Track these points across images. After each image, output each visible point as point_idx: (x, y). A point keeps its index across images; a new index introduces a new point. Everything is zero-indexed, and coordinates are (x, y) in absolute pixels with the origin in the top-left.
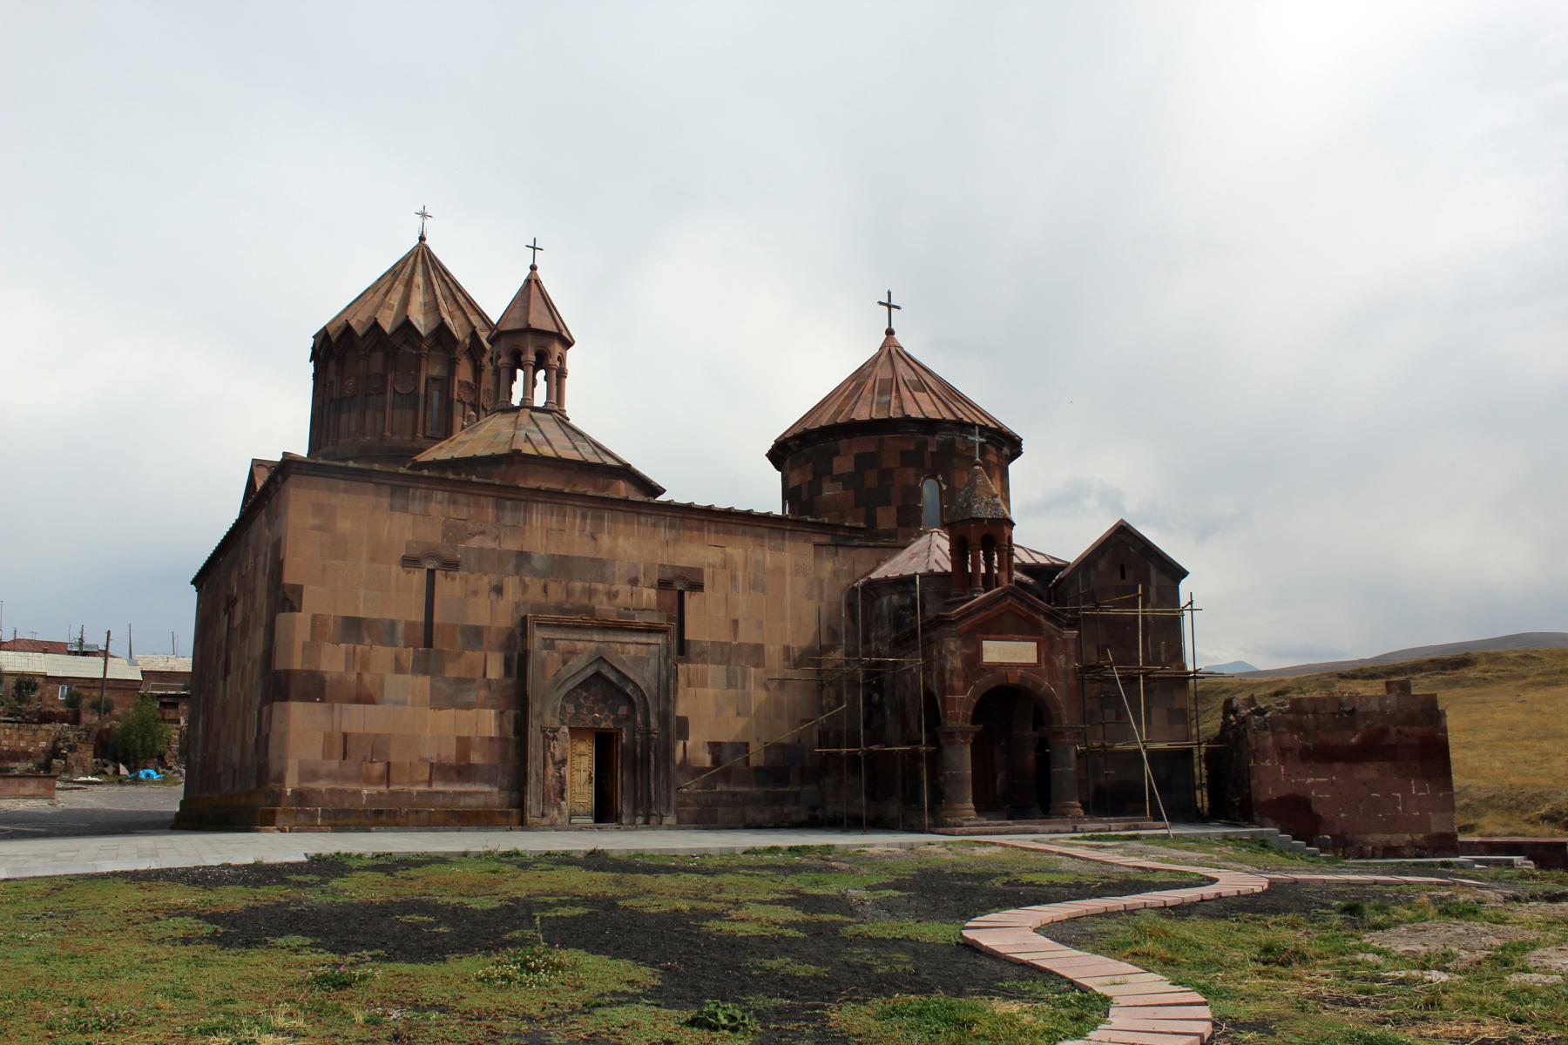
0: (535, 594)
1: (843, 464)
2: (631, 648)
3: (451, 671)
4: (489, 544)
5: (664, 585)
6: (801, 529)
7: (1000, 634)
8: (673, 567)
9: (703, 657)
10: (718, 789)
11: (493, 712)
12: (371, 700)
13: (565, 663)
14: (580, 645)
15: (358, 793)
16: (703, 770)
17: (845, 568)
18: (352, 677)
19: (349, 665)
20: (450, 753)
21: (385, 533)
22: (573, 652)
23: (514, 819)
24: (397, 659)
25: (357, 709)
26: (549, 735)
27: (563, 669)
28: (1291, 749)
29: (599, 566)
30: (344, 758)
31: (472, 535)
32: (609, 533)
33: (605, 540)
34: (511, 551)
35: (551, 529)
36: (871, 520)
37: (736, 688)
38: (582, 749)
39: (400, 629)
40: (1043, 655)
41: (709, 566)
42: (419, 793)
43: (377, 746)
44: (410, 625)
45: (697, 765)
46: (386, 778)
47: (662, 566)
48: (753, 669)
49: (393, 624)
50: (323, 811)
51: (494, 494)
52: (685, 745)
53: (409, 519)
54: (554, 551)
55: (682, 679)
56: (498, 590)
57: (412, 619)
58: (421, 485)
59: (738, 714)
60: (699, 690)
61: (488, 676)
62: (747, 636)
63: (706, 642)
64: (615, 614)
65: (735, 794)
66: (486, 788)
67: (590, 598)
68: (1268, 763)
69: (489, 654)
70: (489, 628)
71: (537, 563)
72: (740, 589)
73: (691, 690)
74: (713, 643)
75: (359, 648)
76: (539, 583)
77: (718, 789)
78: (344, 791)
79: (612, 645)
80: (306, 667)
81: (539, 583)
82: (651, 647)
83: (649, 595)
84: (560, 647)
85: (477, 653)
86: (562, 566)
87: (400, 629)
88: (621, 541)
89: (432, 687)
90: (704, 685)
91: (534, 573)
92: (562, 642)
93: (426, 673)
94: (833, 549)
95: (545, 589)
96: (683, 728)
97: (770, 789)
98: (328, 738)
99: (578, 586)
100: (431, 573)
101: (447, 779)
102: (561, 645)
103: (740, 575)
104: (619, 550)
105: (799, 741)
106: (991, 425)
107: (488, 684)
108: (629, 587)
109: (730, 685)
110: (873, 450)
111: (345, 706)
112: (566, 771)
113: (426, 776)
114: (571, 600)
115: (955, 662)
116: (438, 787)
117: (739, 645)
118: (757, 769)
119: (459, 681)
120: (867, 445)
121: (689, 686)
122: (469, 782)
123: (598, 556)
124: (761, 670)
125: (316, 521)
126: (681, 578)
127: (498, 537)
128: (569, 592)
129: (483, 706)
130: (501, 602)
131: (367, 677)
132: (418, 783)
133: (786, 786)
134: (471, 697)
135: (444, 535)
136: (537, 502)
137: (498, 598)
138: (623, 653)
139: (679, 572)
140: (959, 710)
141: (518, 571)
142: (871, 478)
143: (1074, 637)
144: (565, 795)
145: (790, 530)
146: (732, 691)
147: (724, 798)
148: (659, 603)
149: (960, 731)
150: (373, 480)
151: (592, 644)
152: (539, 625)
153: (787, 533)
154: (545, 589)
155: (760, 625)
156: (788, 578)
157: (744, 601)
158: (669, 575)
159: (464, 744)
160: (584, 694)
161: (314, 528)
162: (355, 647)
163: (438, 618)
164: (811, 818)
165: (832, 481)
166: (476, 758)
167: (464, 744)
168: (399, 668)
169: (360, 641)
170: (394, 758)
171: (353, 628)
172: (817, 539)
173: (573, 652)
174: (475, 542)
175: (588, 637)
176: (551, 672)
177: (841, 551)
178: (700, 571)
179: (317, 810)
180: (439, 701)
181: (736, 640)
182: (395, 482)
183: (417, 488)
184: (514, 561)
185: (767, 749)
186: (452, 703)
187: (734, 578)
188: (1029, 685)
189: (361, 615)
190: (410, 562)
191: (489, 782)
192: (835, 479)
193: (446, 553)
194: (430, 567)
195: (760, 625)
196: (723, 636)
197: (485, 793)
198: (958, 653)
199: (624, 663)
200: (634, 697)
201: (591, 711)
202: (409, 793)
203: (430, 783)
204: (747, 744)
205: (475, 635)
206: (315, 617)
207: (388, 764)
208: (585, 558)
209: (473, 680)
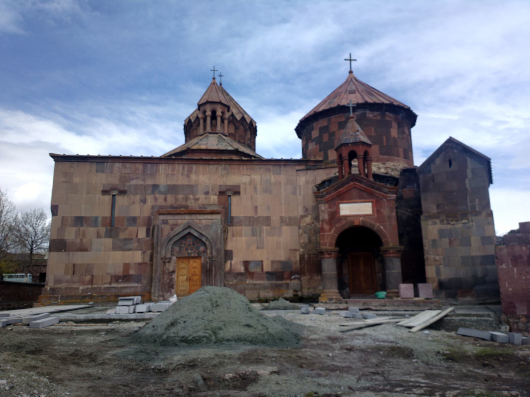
0: (161, 202)
1: (315, 134)
3: (122, 236)
4: (140, 182)
5: (222, 193)
7: (350, 200)
8: (226, 186)
9: (240, 224)
10: (248, 282)
11: (140, 252)
12: (86, 250)
13: (172, 229)
14: (180, 222)
15: (78, 288)
16: (240, 274)
17: (311, 179)
18: (78, 241)
20: (119, 271)
22: (176, 225)
25: (80, 254)
26: (166, 261)
28: (521, 257)
29: (191, 188)
31: (133, 179)
32: (195, 173)
33: (193, 177)
34: (149, 185)
35: (169, 174)
36: (326, 156)
37: (257, 236)
39: (100, 220)
41: (243, 184)
42: (105, 288)
43: (88, 269)
44: (104, 218)
46: (91, 282)
47: (220, 186)
48: (265, 228)
49: (96, 218)
50: (61, 296)
53: (104, 175)
54: (169, 183)
55: (230, 234)
56: (144, 201)
58: (109, 161)
59: (258, 248)
60: (238, 238)
62: (262, 213)
63: (242, 217)
65: (255, 285)
66: (136, 285)
67: (186, 202)
68: (504, 266)
70: (139, 217)
71: (162, 189)
72: (259, 193)
73: (235, 238)
74: (245, 217)
75: (81, 228)
76: (163, 196)
77: (248, 282)
78: (72, 288)
79: (195, 221)
80: (59, 238)
81: (163, 196)
83: (214, 198)
86: (173, 189)
87: (100, 220)
89: (113, 243)
90: (241, 235)
91: (160, 193)
92: (172, 221)
93: (110, 237)
94: (305, 172)
95: (165, 199)
96: (228, 255)
97: (274, 282)
98: (67, 266)
99: (180, 196)
100: (114, 196)
102: (171, 222)
103: (258, 187)
106: (386, 102)
107: (139, 240)
108: (204, 196)
109: (253, 235)
110: (326, 124)
111: (75, 253)
112: (174, 276)
113: (109, 281)
117: (258, 217)
118: (268, 273)
119: (125, 240)
120: (323, 122)
121: (233, 236)
123: (190, 184)
124: (269, 228)
125: (64, 179)
126: (228, 190)
128: (177, 200)
129: (136, 249)
130: (145, 206)
131: (85, 241)
132: (105, 283)
133: (282, 280)
134: (131, 246)
135: (120, 180)
136: (162, 163)
138: (200, 223)
141: (153, 192)
142: (326, 138)
143: (394, 198)
145: (284, 165)
146: (255, 238)
147: (250, 286)
148: (219, 201)
149: (327, 251)
150: (88, 161)
152: (160, 214)
153: (282, 167)
154: (165, 199)
155: (269, 208)
156: (283, 187)
157: (260, 199)
158: (224, 189)
160: (184, 242)
161: (64, 182)
162: (80, 229)
163: (117, 214)
164: (296, 295)
165: (312, 142)
166: (132, 272)
167: (127, 266)
168: (99, 236)
169: (82, 226)
170: (95, 273)
171: (79, 221)
173: (176, 225)
174: (134, 182)
175: (184, 218)
176: (165, 233)
177: (309, 172)
178: (238, 186)
179: (58, 296)
180: (115, 248)
181: (256, 215)
183: (108, 162)
184: (151, 189)
185: (273, 262)
186: (122, 249)
187: (255, 188)
188: (368, 225)
189: (83, 215)
190: (105, 192)
192: (312, 141)
193: (121, 188)
194: (114, 193)
195: (269, 208)
196: (250, 213)
197: (134, 287)
198: (326, 211)
199: (200, 228)
200: (207, 243)
201: (187, 249)
202: (100, 288)
204: (262, 262)
205: (133, 220)
206: (63, 218)
207: (93, 276)
208: (184, 185)
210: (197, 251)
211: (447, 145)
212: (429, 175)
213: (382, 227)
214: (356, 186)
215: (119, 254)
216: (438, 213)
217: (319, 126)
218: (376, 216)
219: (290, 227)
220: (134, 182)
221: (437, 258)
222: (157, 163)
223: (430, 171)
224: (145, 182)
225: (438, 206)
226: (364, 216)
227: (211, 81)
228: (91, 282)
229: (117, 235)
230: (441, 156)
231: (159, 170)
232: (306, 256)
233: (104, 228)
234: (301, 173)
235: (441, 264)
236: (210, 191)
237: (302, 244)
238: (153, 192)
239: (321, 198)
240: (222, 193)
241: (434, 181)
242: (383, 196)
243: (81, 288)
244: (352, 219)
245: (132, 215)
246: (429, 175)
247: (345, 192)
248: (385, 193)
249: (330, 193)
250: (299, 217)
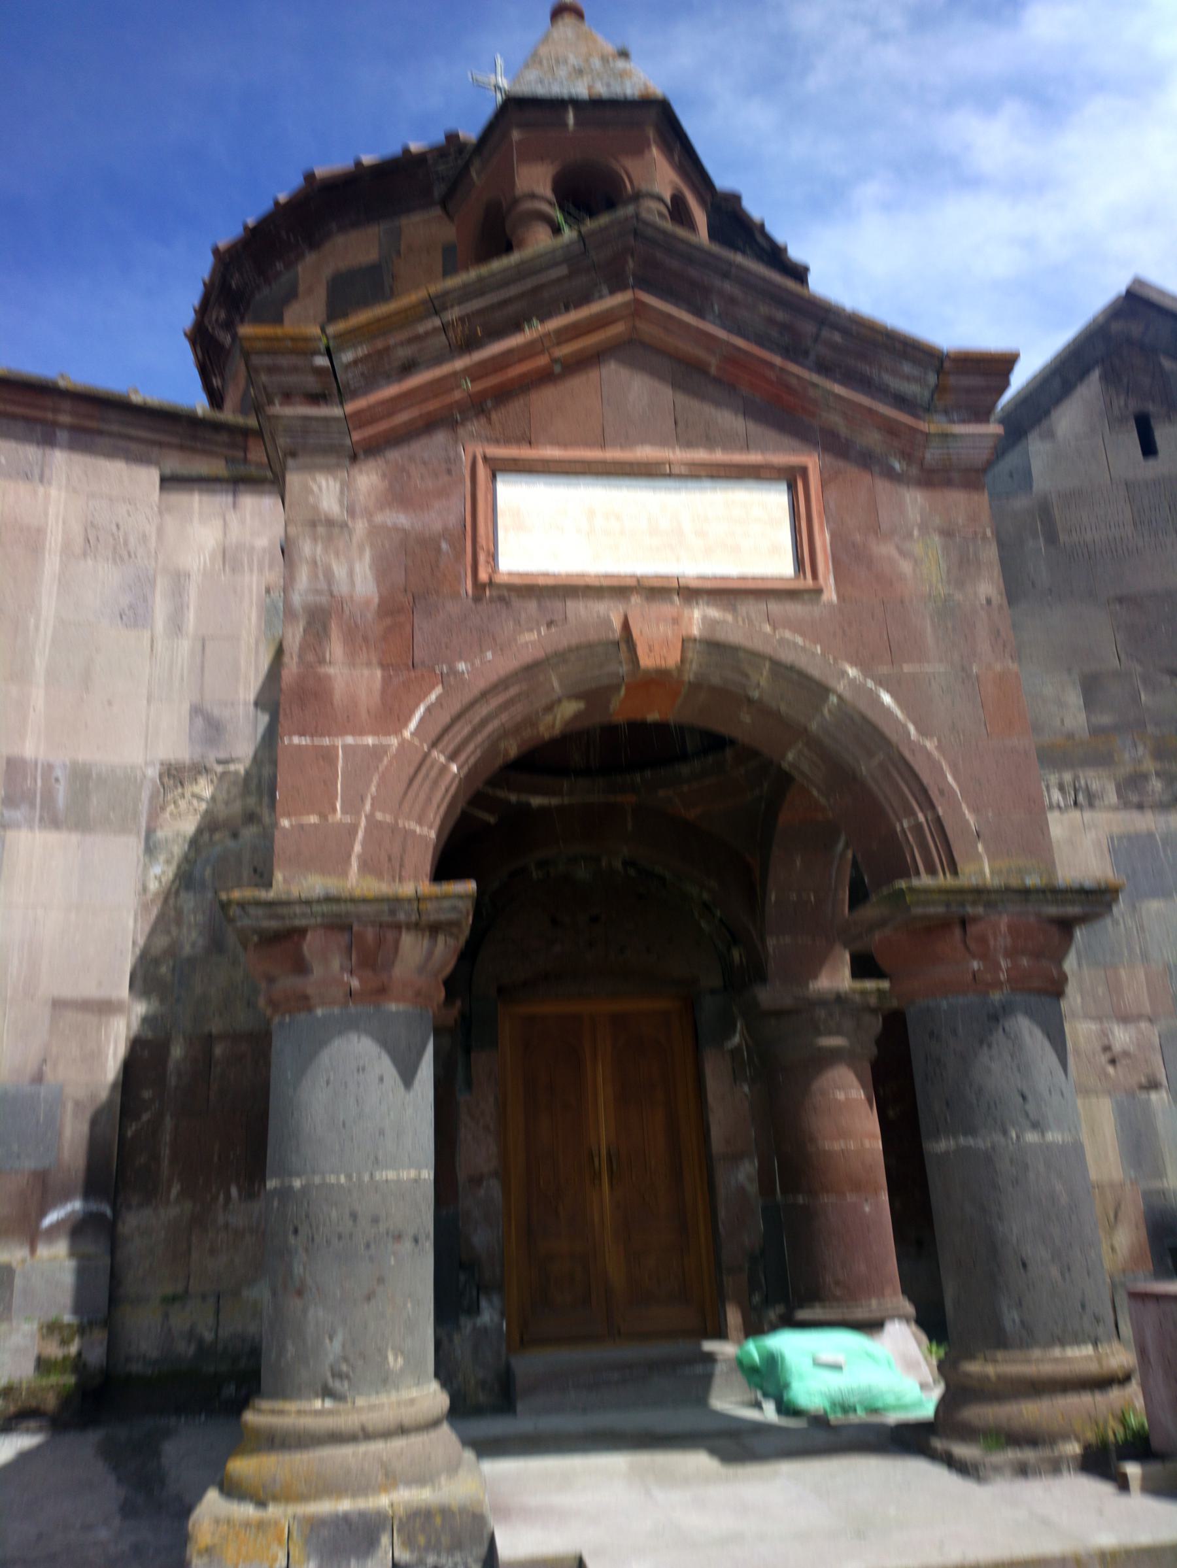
6: (115, 428)
17: (262, 542)
40: (823, 540)
105: (38, 1078)
115: (340, 571)
140: (353, 806)
145: (74, 429)
156: (51, 563)
172: (175, 463)
198: (360, 527)
211: (1116, 327)
212: (1021, 503)
213: (887, 699)
214: (647, 329)
216: (1096, 731)
217: (327, 272)
218: (830, 594)
219: (74, 838)
221: (1122, 1037)
223: (1025, 477)
225: (1091, 688)
230: (1091, 389)
232: (177, 1051)
234: (195, 501)
235: (1153, 1085)
237: (156, 962)
239: (316, 398)
241: (1052, 538)
242: (891, 429)
244: (612, 613)
246: (1021, 503)
248: (901, 401)
249: (408, 368)
250: (152, 772)
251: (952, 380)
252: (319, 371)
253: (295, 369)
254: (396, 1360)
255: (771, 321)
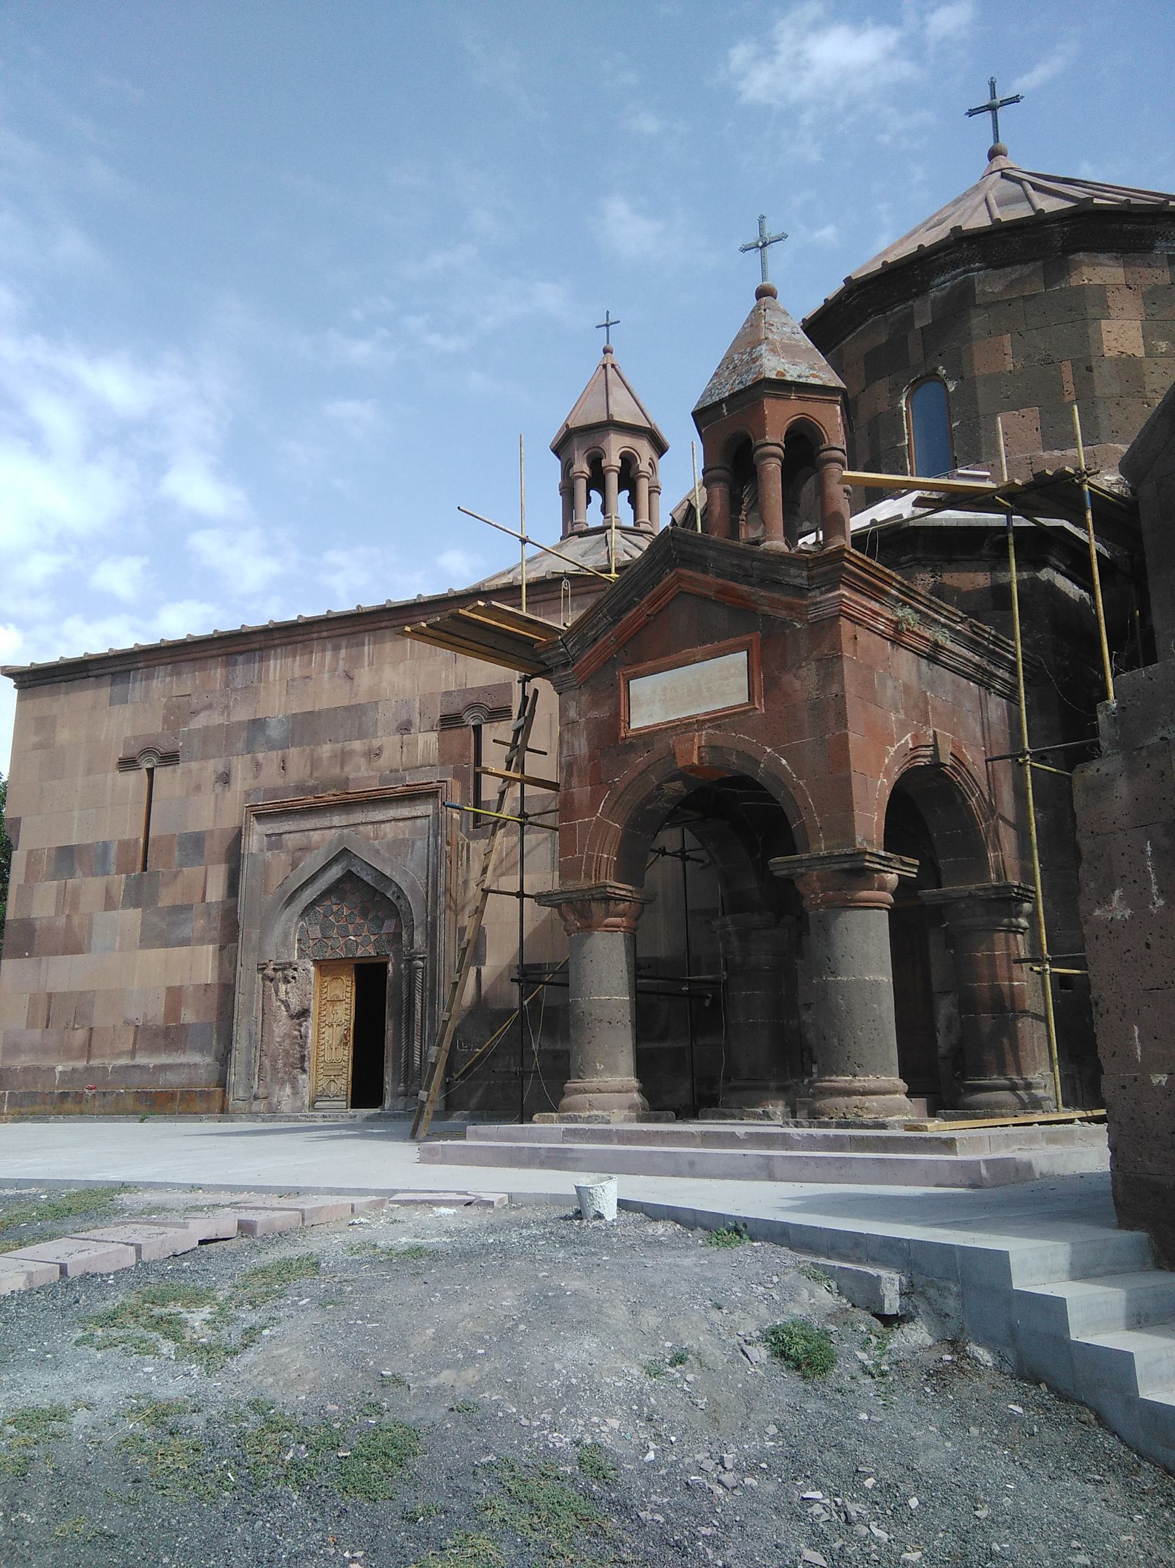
0: (271, 776)
2: (387, 827)
4: (216, 718)
13: (294, 865)
18: (63, 920)
19: (59, 906)
20: (156, 1012)
21: (103, 737)
23: (216, 1105)
24: (107, 891)
27: (291, 875)
30: (47, 1027)
31: (195, 713)
32: (371, 664)
33: (364, 677)
34: (240, 723)
35: (293, 680)
38: (337, 992)
39: (113, 853)
42: (116, 1069)
44: (124, 845)
45: (498, 1007)
46: (88, 1050)
47: (447, 694)
49: (106, 845)
51: (221, 651)
52: (479, 972)
54: (296, 710)
56: (225, 779)
57: (126, 837)
61: (208, 900)
64: (376, 781)
67: (342, 767)
69: (209, 867)
70: (211, 832)
76: (275, 755)
79: (361, 828)
82: (418, 821)
83: (427, 742)
84: (289, 843)
85: (195, 869)
87: (113, 853)
88: (388, 673)
91: (271, 745)
93: (136, 906)
98: (33, 999)
100: (150, 772)
101: (154, 1049)
104: (384, 685)
108: (397, 737)
114: (316, 774)
115: (576, 744)
116: (141, 1060)
122: (176, 1051)
126: (471, 707)
127: (227, 707)
128: (315, 763)
129: (201, 941)
131: (76, 920)
132: (119, 1055)
134: (186, 931)
135: (166, 720)
136: (274, 647)
137: (223, 790)
139: (472, 699)
141: (250, 749)
144: (306, 1064)
151: (333, 831)
158: (457, 705)
159: (175, 996)
166: (188, 1016)
168: (109, 904)
174: (198, 723)
175: (327, 823)
179: (5, 1093)
180: (151, 938)
182: (112, 670)
184: (244, 735)
186: (167, 941)
190: (127, 764)
191: (201, 1050)
193: (165, 746)
194: (149, 766)
203: (133, 1056)
206: (30, 852)
209: (189, 907)
210: (373, 938)
213: (784, 762)
214: (685, 586)
215: (158, 954)
220: (198, 723)
222: (261, 649)
224: (228, 715)
226: (716, 720)
227: (600, 358)
228: (88, 1050)
229: (153, 899)
231: (267, 671)
233: (123, 876)
236: (416, 719)
238: (250, 749)
240: (449, 722)
243: (60, 1068)
245: (193, 828)
247: (645, 625)
251: (814, 572)
252: (562, 654)
253: (555, 656)
254: (600, 1066)
255: (732, 565)
